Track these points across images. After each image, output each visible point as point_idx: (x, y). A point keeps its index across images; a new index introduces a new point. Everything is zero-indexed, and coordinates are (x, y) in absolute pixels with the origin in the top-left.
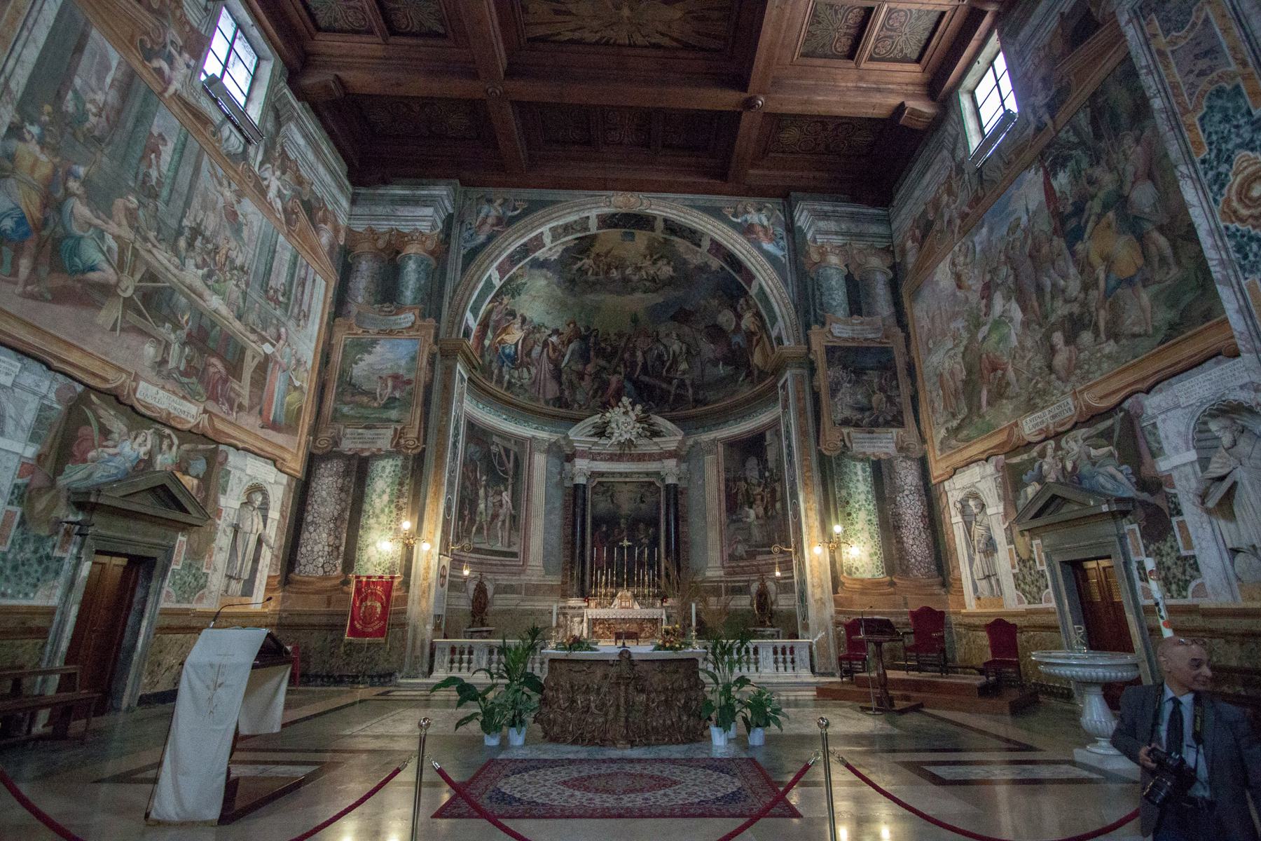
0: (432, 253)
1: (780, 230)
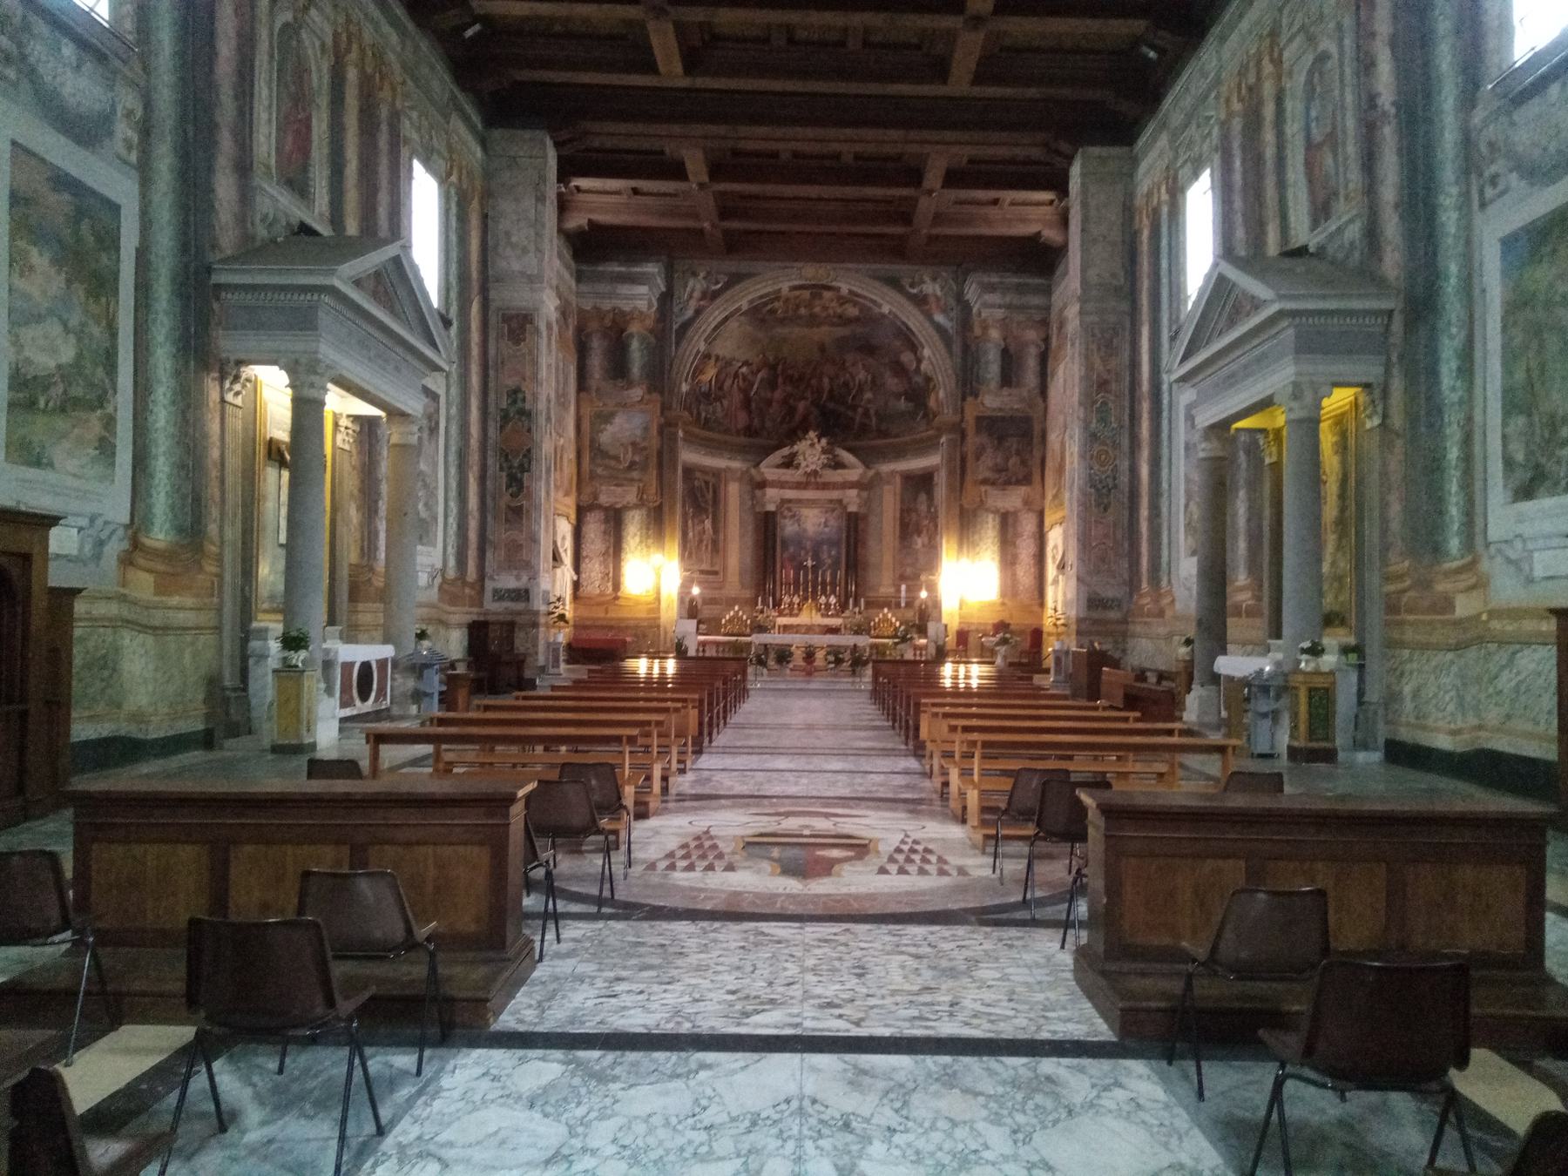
0: (651, 331)
1: (952, 302)
